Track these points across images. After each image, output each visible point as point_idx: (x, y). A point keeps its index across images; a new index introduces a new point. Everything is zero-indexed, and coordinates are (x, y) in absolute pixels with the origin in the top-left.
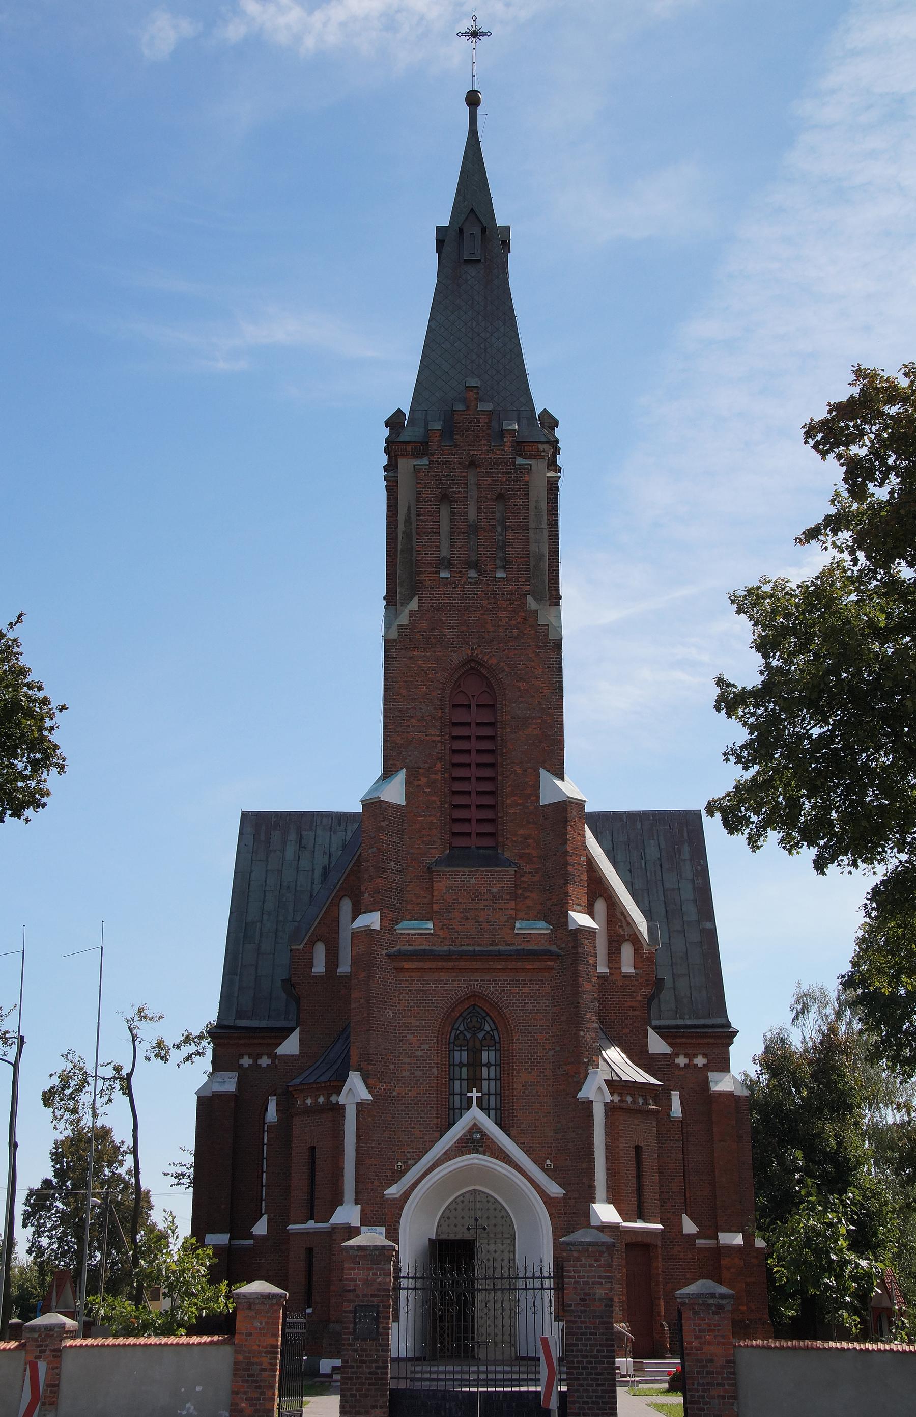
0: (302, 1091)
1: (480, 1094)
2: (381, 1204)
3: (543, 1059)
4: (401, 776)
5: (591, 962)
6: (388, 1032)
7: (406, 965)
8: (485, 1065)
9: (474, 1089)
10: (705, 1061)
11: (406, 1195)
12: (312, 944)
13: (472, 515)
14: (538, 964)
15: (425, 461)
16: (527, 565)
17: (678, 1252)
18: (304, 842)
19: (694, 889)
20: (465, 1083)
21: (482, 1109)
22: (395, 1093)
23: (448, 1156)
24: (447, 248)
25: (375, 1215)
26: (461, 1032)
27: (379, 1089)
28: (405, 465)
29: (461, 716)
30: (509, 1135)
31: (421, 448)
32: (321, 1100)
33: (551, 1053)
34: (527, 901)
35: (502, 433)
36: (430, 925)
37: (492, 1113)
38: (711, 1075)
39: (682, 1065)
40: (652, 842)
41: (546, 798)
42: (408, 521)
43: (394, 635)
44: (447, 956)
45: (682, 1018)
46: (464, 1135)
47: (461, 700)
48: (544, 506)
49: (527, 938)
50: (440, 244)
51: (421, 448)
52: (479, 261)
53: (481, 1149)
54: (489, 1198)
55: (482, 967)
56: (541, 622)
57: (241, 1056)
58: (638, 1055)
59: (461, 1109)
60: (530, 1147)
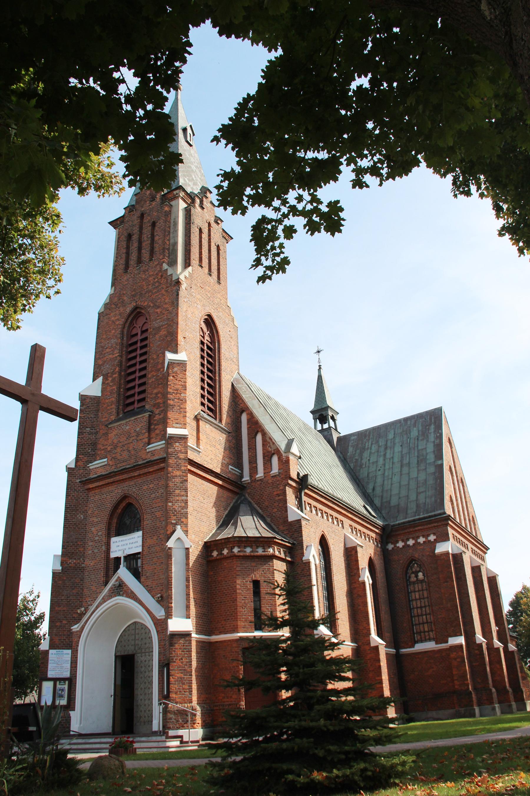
2: (68, 635)
3: (159, 528)
4: (100, 380)
5: (181, 457)
7: (91, 486)
10: (435, 537)
14: (156, 467)
19: (434, 446)
23: (104, 600)
25: (63, 642)
27: (70, 563)
30: (140, 582)
34: (156, 431)
39: (422, 542)
40: (415, 429)
45: (419, 515)
49: (153, 453)
53: (121, 593)
54: (143, 626)
55: (127, 477)
60: (151, 587)
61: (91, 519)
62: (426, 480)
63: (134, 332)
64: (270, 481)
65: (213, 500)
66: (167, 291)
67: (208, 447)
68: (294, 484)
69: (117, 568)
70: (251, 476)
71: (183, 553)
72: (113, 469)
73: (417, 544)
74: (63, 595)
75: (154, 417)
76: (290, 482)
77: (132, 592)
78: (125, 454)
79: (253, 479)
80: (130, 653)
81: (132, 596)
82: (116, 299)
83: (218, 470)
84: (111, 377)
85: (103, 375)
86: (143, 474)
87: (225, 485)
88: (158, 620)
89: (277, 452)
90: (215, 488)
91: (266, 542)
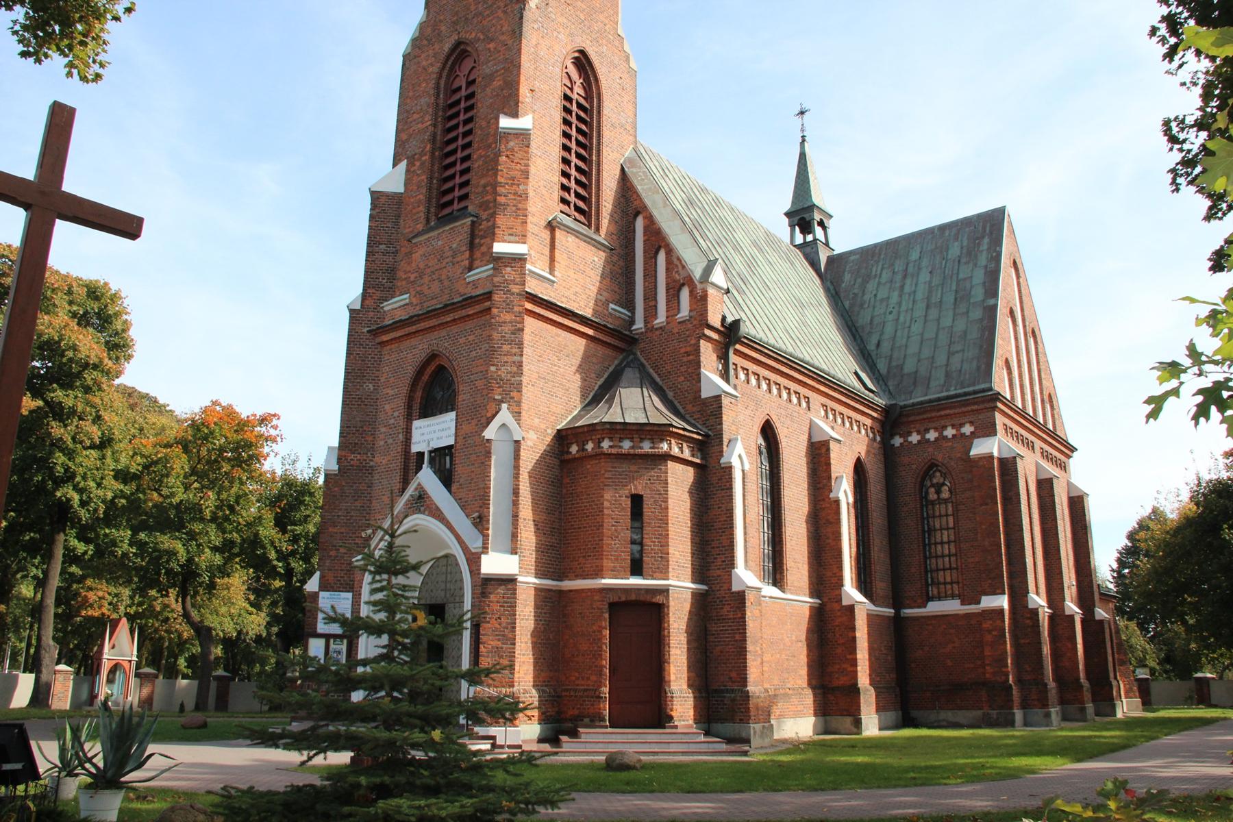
2: (348, 571)
4: (403, 165)
5: (514, 290)
6: (366, 405)
7: (385, 338)
17: (728, 611)
19: (985, 274)
25: (340, 581)
27: (351, 460)
30: (450, 491)
39: (950, 436)
40: (956, 244)
45: (948, 390)
49: (475, 284)
53: (422, 509)
55: (436, 323)
61: (385, 391)
62: (965, 333)
63: (455, 86)
64: (675, 331)
65: (577, 360)
66: (505, 12)
67: (571, 273)
68: (715, 336)
69: (419, 468)
70: (646, 322)
71: (510, 448)
72: (417, 311)
73: (942, 438)
74: (341, 510)
75: (480, 225)
76: (707, 332)
77: (438, 509)
78: (436, 287)
79: (649, 329)
80: (439, 601)
81: (438, 514)
83: (588, 313)
84: (419, 159)
85: (407, 158)
86: (459, 319)
87: (600, 336)
88: (473, 554)
89: (689, 281)
90: (583, 342)
91: (658, 432)
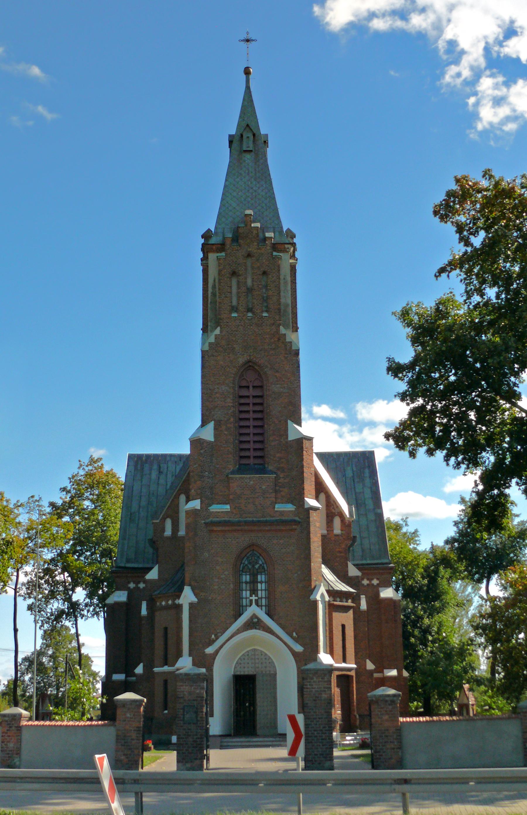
0: (160, 598)
1: (257, 598)
4: (211, 425)
7: (215, 528)
8: (260, 582)
9: (254, 595)
11: (217, 652)
12: (164, 520)
13: (249, 282)
14: (288, 527)
15: (223, 254)
16: (279, 310)
18: (162, 470)
20: (248, 592)
21: (258, 606)
22: (210, 598)
24: (235, 145)
26: (246, 565)
28: (212, 257)
29: (244, 392)
30: (273, 620)
31: (221, 247)
32: (170, 602)
33: (296, 575)
34: (282, 493)
35: (265, 239)
36: (228, 507)
37: (264, 608)
38: (380, 589)
40: (349, 468)
41: (291, 437)
42: (214, 287)
43: (207, 348)
44: (239, 523)
45: (366, 559)
46: (249, 620)
47: (244, 384)
48: (289, 279)
49: (282, 513)
50: (231, 142)
51: (221, 247)
52: (251, 151)
53: (257, 627)
56: (287, 340)
57: (129, 583)
58: (343, 576)
59: (246, 606)
75: (279, 479)
80: (251, 673)
82: (224, 342)
85: (215, 420)
88: (296, 652)
